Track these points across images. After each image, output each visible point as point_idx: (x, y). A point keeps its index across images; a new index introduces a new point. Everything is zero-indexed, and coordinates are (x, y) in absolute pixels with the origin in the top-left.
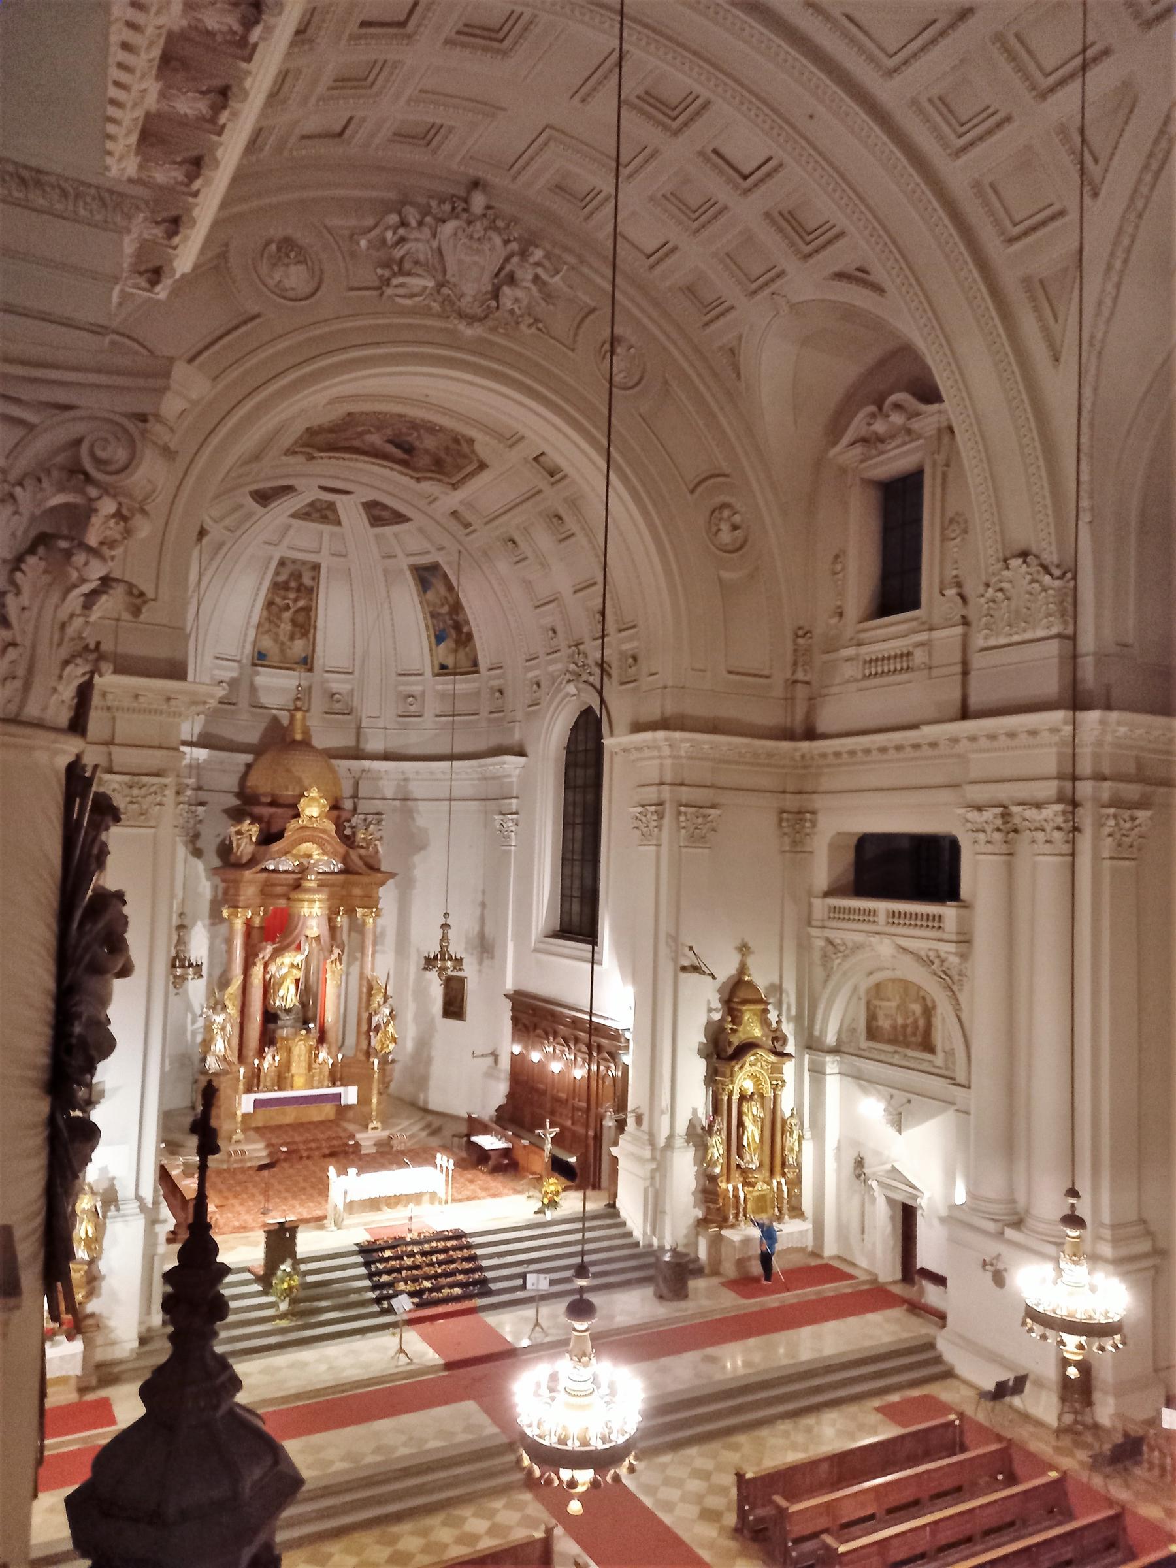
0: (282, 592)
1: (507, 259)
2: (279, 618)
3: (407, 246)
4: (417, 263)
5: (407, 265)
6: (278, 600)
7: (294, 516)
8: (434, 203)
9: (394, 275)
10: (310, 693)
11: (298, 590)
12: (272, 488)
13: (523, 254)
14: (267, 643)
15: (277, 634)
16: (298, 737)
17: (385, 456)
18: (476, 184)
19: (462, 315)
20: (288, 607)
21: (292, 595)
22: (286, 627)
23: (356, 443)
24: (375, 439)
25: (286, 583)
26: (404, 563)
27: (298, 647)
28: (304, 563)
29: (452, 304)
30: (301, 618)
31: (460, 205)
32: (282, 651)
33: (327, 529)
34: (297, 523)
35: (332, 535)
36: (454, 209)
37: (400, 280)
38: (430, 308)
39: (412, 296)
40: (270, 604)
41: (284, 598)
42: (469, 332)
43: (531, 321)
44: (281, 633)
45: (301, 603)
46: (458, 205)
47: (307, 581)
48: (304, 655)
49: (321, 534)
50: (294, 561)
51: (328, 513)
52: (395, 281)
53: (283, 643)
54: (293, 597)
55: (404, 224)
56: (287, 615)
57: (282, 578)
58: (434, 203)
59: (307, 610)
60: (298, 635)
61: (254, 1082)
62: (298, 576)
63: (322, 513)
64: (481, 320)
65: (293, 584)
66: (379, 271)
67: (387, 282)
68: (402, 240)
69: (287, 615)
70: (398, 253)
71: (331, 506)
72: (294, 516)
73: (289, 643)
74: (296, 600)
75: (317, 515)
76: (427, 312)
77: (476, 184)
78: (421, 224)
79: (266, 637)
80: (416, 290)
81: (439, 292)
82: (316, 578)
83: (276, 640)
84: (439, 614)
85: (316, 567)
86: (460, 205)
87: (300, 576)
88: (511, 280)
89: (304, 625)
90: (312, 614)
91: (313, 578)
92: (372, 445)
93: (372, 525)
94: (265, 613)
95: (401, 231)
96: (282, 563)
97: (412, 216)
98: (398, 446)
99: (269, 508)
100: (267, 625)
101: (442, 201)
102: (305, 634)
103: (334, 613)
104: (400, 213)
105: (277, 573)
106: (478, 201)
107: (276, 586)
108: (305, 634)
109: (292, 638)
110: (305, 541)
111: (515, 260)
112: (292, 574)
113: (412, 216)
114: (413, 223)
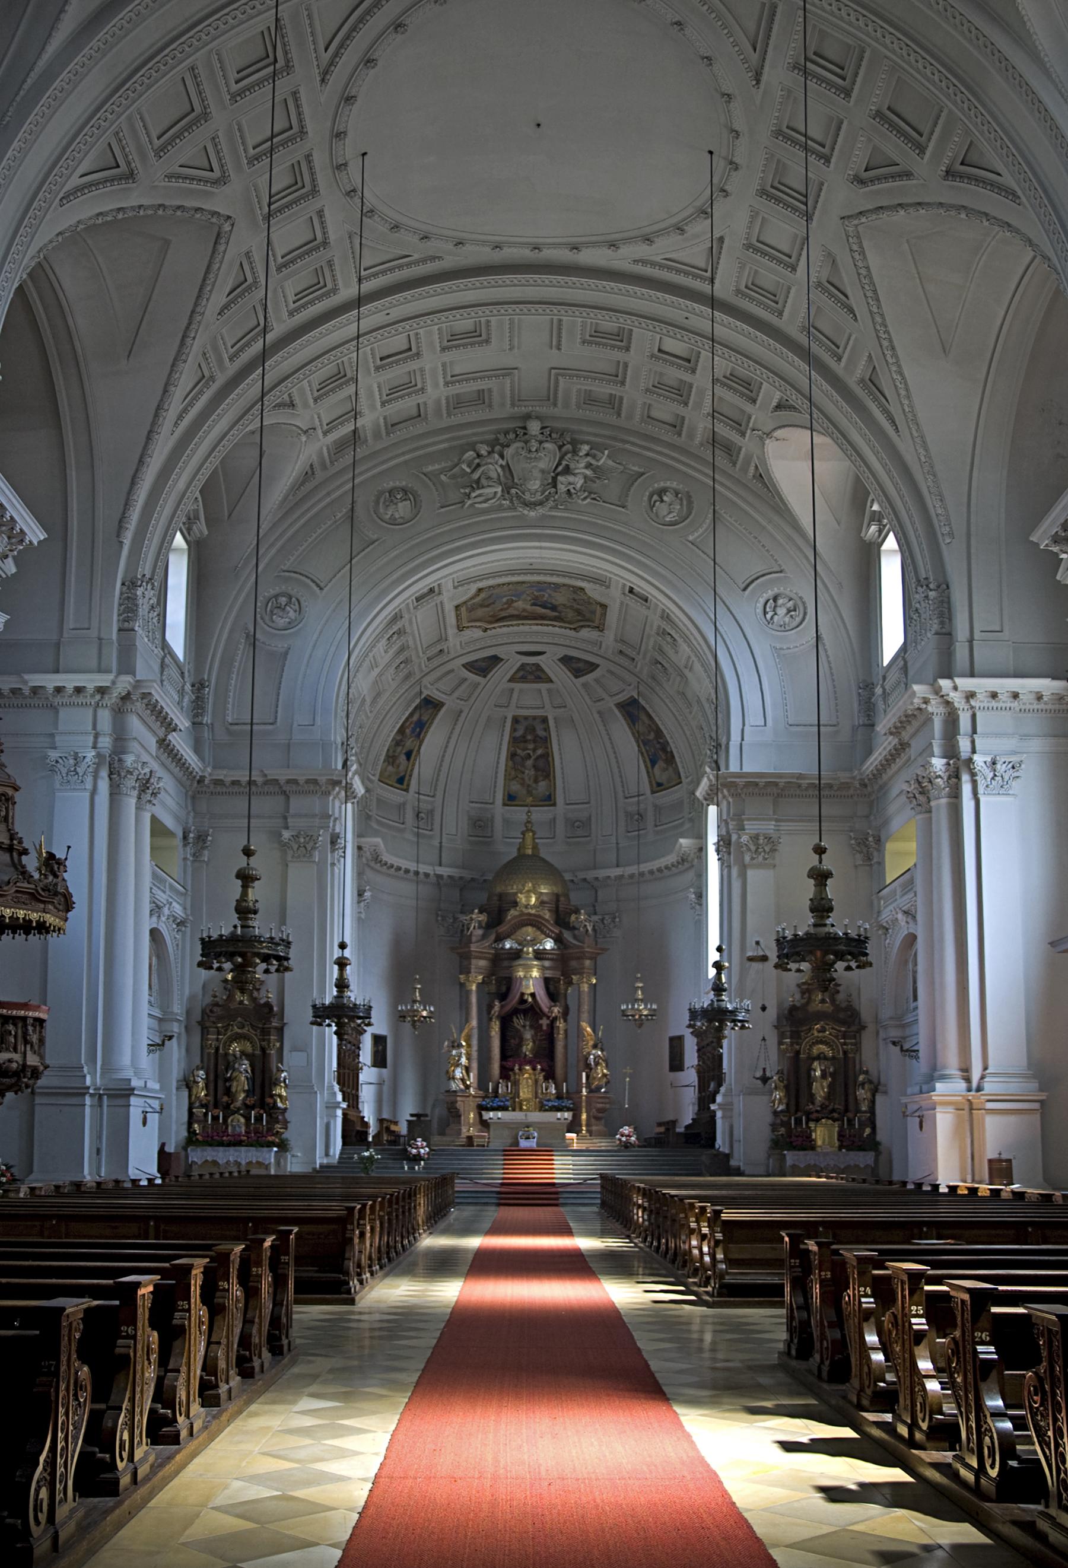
0: (522, 745)
1: (562, 458)
2: (523, 766)
3: (481, 469)
4: (489, 478)
5: (484, 482)
6: (519, 751)
8: (501, 437)
9: (473, 490)
11: (535, 741)
12: (484, 659)
14: (515, 787)
15: (523, 779)
16: (529, 852)
17: (543, 617)
18: (528, 417)
19: (527, 504)
20: (529, 756)
21: (531, 746)
22: (530, 772)
23: (511, 611)
24: (520, 604)
25: (524, 736)
27: (542, 785)
28: (535, 718)
29: (518, 497)
30: (541, 763)
31: (520, 432)
32: (530, 793)
33: (543, 687)
34: (517, 686)
35: (549, 691)
36: (517, 435)
37: (478, 492)
38: (501, 505)
39: (485, 501)
40: (512, 756)
41: (524, 749)
43: (586, 494)
44: (526, 778)
45: (539, 752)
46: (521, 433)
47: (541, 733)
49: (540, 691)
50: (526, 718)
51: (539, 673)
52: (473, 495)
53: (529, 786)
54: (530, 750)
55: (479, 456)
58: (501, 437)
59: (547, 757)
62: (531, 729)
63: (530, 674)
65: (529, 737)
66: (462, 491)
67: (468, 496)
68: (478, 465)
70: (476, 476)
71: (537, 666)
73: (534, 785)
74: (534, 750)
75: (530, 677)
76: (500, 508)
78: (489, 453)
79: (514, 782)
80: (491, 496)
81: (508, 493)
82: (547, 729)
83: (522, 784)
84: (649, 741)
85: (545, 720)
86: (520, 432)
87: (534, 730)
89: (545, 769)
90: (550, 759)
91: (545, 730)
92: (524, 610)
93: (576, 677)
94: (510, 763)
95: (477, 461)
96: (516, 720)
97: (484, 450)
98: (544, 607)
99: (489, 676)
100: (513, 773)
101: (506, 433)
103: (568, 754)
104: (475, 451)
105: (514, 730)
109: (536, 781)
110: (529, 700)
111: (569, 455)
112: (526, 729)
113: (484, 450)
114: (484, 452)
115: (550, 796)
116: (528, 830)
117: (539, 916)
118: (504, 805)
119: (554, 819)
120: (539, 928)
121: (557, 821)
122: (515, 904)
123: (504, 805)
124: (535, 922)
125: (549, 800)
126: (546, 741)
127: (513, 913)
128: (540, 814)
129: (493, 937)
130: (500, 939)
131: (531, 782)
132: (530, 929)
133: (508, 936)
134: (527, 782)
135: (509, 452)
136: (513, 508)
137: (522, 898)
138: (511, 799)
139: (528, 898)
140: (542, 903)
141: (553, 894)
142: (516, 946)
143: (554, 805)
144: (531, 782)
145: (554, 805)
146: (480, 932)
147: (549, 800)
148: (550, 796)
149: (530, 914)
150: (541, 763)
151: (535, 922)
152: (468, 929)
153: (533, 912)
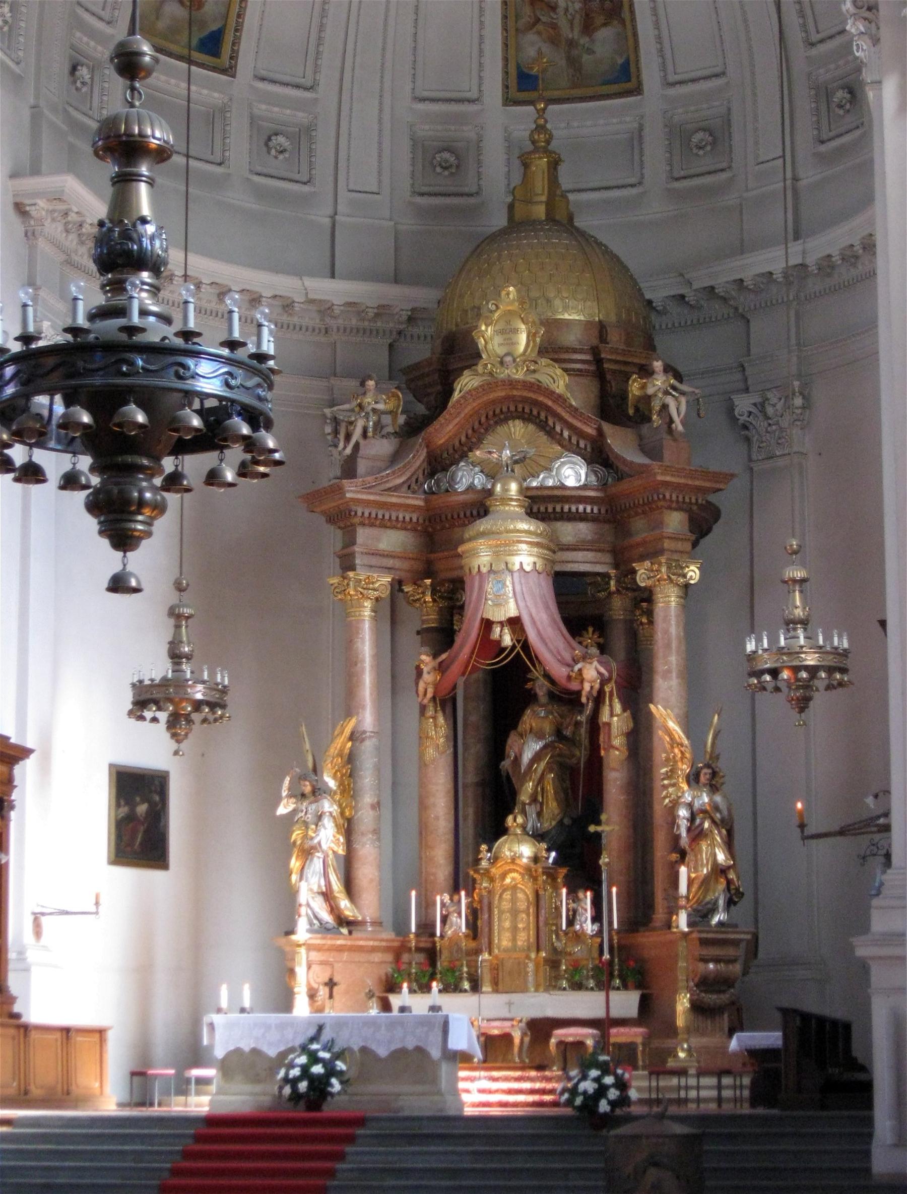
10: (641, 142)
15: (554, 26)
32: (573, 62)
48: (620, 61)
53: (571, 44)
60: (599, 20)
73: (584, 40)
79: (531, 37)
83: (554, 41)
109: (588, 28)
115: (627, 63)
116: (536, 150)
117: (537, 387)
118: (509, 101)
119: (641, 128)
120: (543, 426)
121: (647, 130)
123: (509, 101)
124: (527, 406)
125: (624, 79)
127: (466, 382)
129: (417, 458)
130: (439, 464)
131: (576, 34)
132: (517, 428)
133: (460, 452)
134: (566, 32)
137: (488, 337)
138: (523, 84)
139: (509, 333)
140: (550, 349)
141: (588, 324)
142: (479, 481)
143: (637, 90)
144: (576, 34)
145: (637, 90)
146: (383, 447)
147: (624, 79)
148: (627, 63)
149: (511, 383)
151: (527, 406)
152: (348, 437)
153: (519, 375)
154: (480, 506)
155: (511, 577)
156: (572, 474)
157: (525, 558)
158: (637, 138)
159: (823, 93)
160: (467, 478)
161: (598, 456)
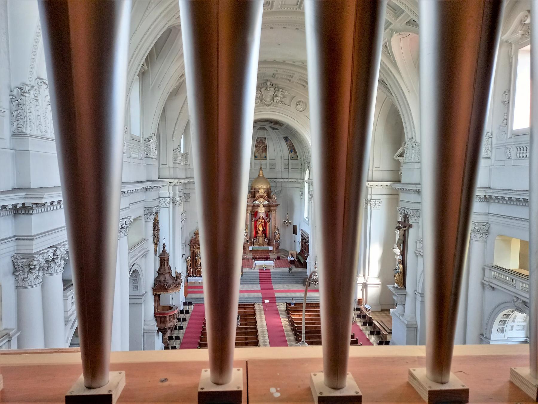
7: (258, 129)
13: (278, 90)
14: (257, 154)
18: (267, 80)
26: (282, 136)
27: (264, 154)
33: (265, 131)
34: (259, 131)
42: (267, 108)
47: (264, 141)
56: (261, 148)
57: (258, 141)
59: (265, 147)
61: (252, 244)
62: (261, 140)
64: (269, 105)
69: (261, 148)
72: (258, 129)
77: (267, 80)
88: (276, 96)
89: (264, 150)
96: (258, 138)
102: (265, 152)
103: (271, 147)
106: (268, 83)
107: (257, 143)
108: (265, 152)
122: (258, 192)
125: (265, 158)
126: (265, 143)
127: (257, 195)
128: (264, 162)
130: (254, 201)
135: (262, 90)
136: (263, 106)
150: (264, 148)
154: (259, 206)
155: (262, 212)
156: (266, 202)
157: (263, 211)
158: (266, 164)
159: (285, 164)
160: (257, 202)
161: (268, 201)
